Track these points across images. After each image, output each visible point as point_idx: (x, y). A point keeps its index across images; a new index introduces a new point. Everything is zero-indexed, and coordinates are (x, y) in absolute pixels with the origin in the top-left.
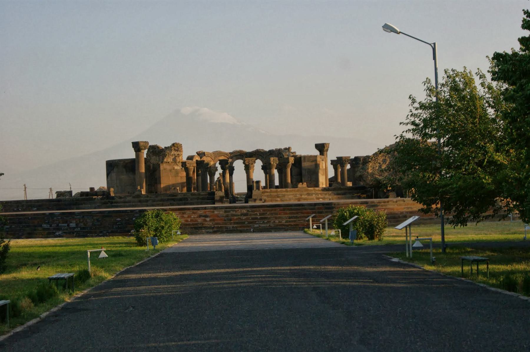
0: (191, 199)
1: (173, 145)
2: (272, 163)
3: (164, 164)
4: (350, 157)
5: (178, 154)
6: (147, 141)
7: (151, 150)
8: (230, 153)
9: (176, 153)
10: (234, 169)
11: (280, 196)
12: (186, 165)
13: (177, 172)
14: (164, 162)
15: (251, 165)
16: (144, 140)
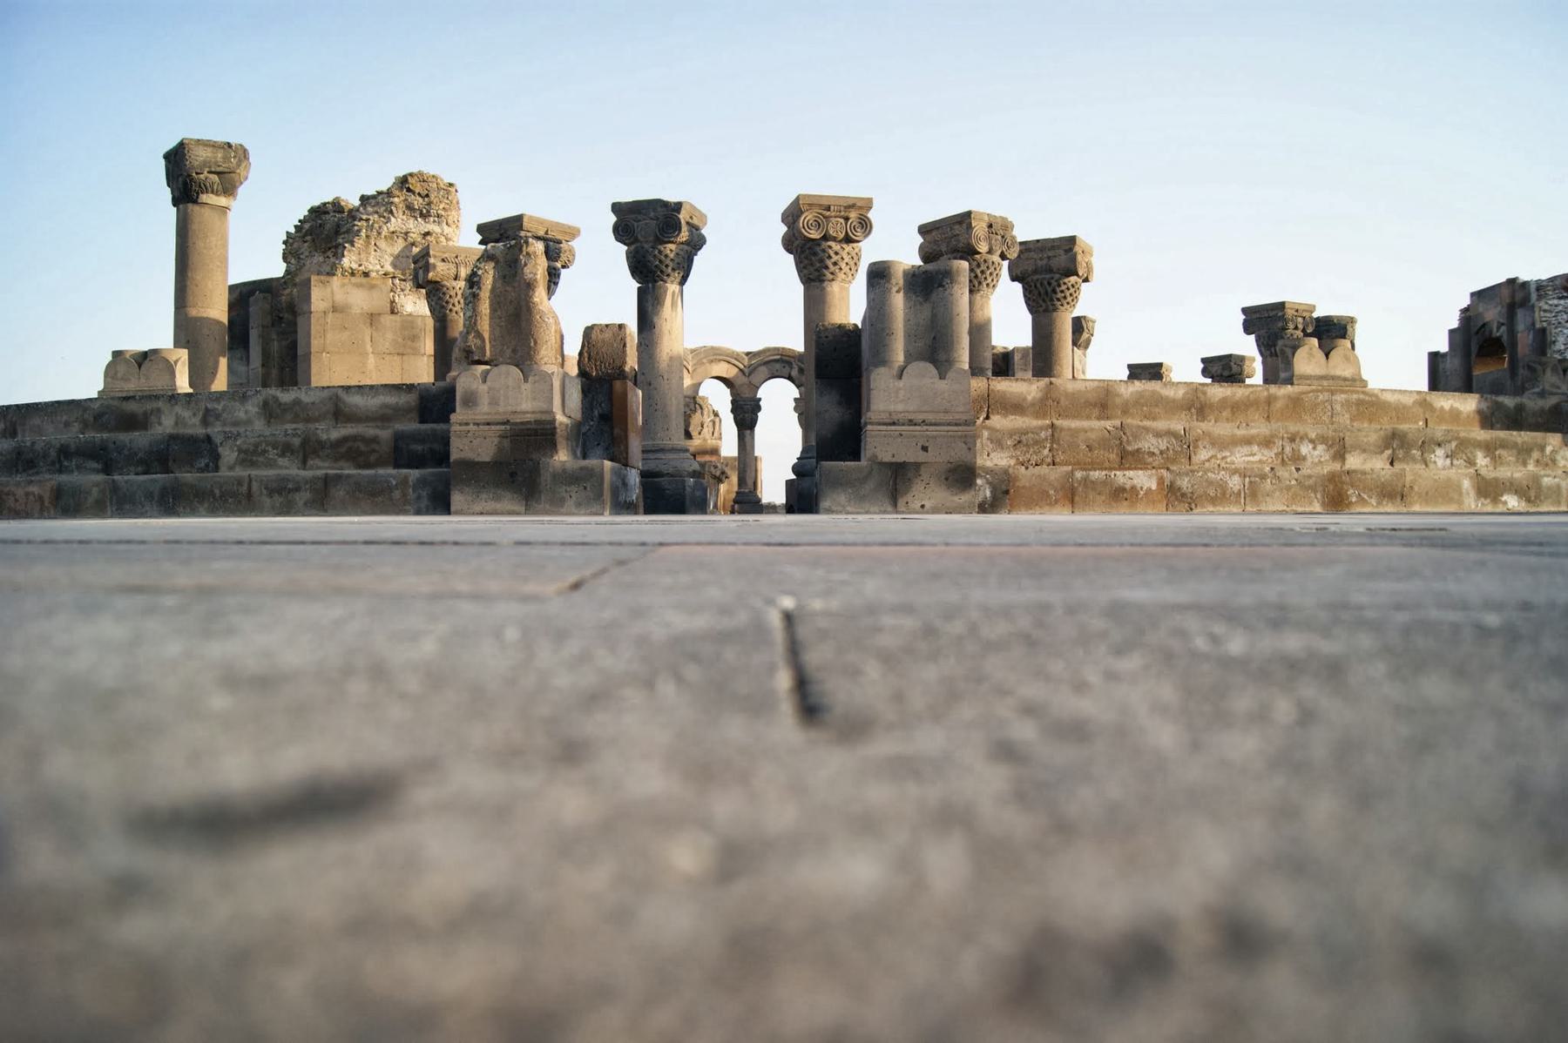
0: (249, 457)
1: (403, 182)
2: (983, 248)
3: (336, 281)
4: (1312, 308)
5: (427, 234)
6: (233, 141)
7: (307, 226)
8: (748, 354)
9: (416, 227)
10: (759, 408)
11: (1149, 444)
12: (427, 267)
13: (409, 327)
14: (339, 272)
15: (836, 246)
16: (220, 138)
